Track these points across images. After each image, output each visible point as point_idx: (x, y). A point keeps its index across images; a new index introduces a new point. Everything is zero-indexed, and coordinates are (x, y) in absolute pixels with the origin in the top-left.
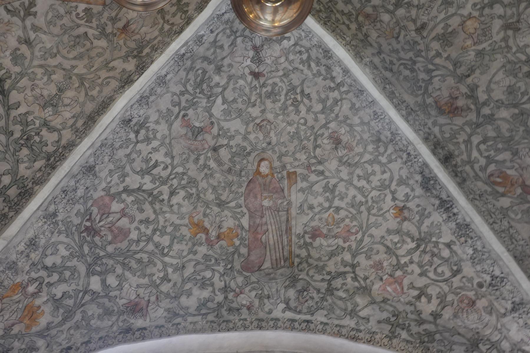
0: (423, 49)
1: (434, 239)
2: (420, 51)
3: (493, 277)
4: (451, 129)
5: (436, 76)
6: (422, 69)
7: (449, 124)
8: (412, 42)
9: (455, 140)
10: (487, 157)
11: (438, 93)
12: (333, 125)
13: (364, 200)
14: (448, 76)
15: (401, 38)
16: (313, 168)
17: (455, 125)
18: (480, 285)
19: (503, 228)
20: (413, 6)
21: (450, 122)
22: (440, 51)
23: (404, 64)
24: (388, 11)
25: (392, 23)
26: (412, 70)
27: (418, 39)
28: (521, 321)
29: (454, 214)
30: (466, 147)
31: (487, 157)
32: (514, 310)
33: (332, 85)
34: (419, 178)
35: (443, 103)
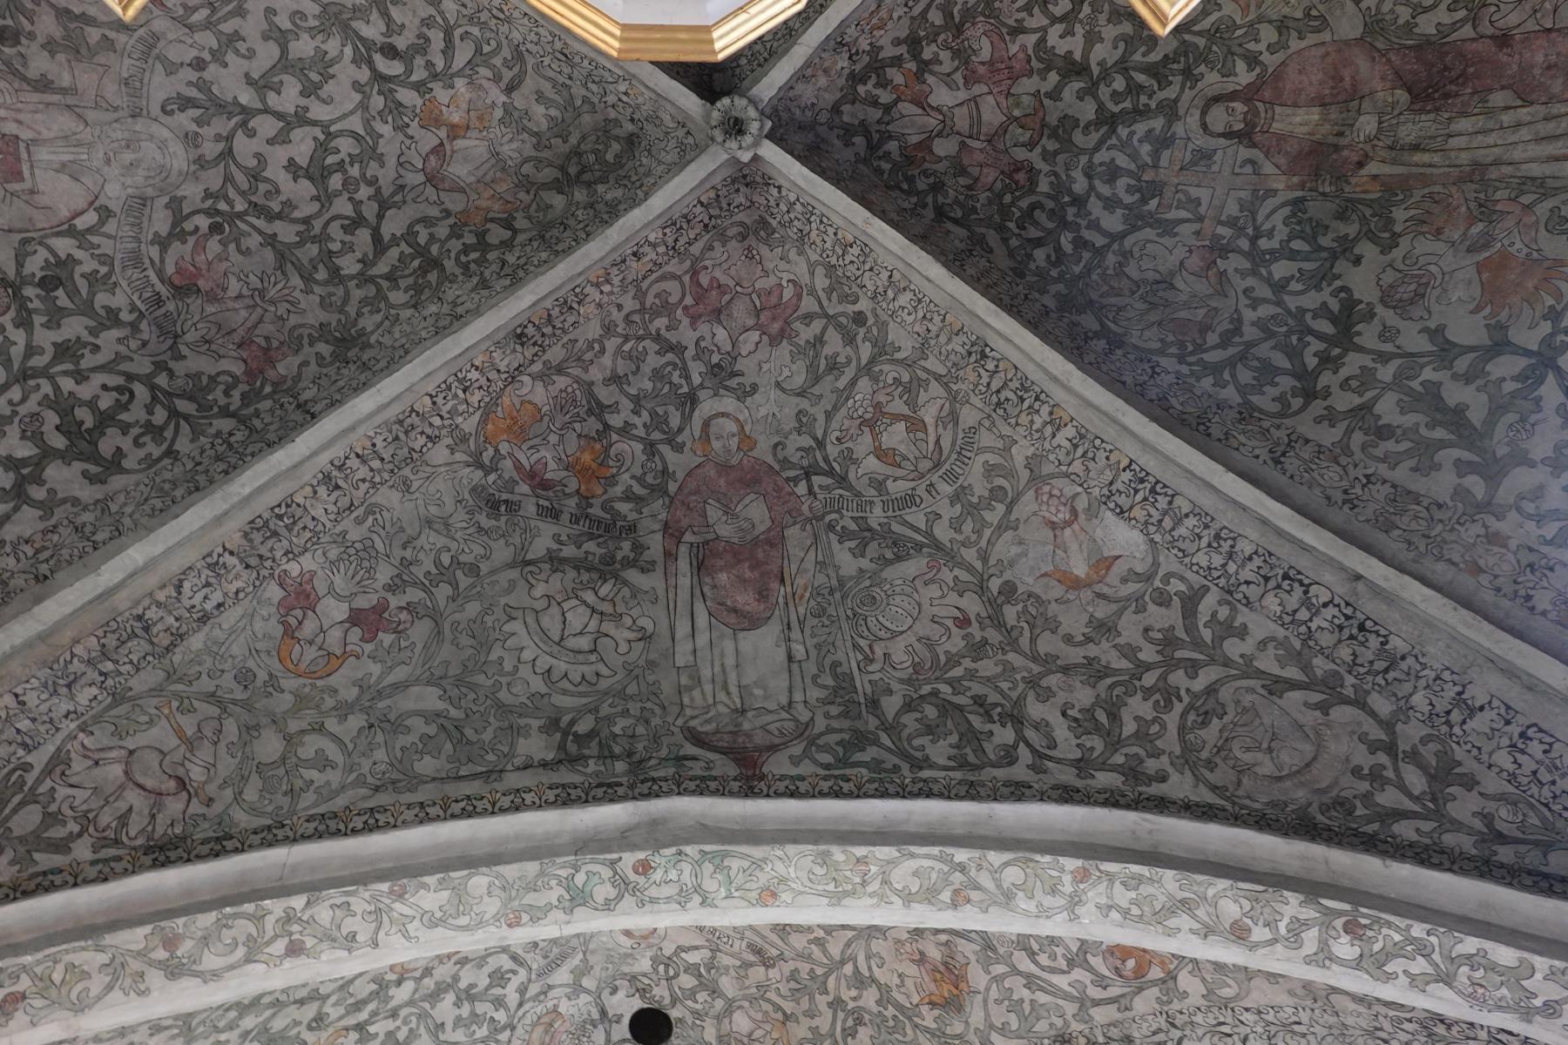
0: (808, 967)
2: (812, 975)
4: (998, 1002)
5: (870, 968)
6: (854, 993)
7: (985, 1001)
8: (793, 985)
9: (1027, 1007)
10: (1071, 963)
11: (909, 983)
14: (868, 946)
15: (788, 1007)
17: (988, 989)
19: (1259, 1029)
20: (713, 958)
21: (979, 997)
22: (812, 937)
23: (844, 1030)
24: (729, 1010)
25: (752, 1013)
26: (859, 1022)
27: (787, 968)
30: (1042, 989)
31: (1071, 963)
35: (933, 987)
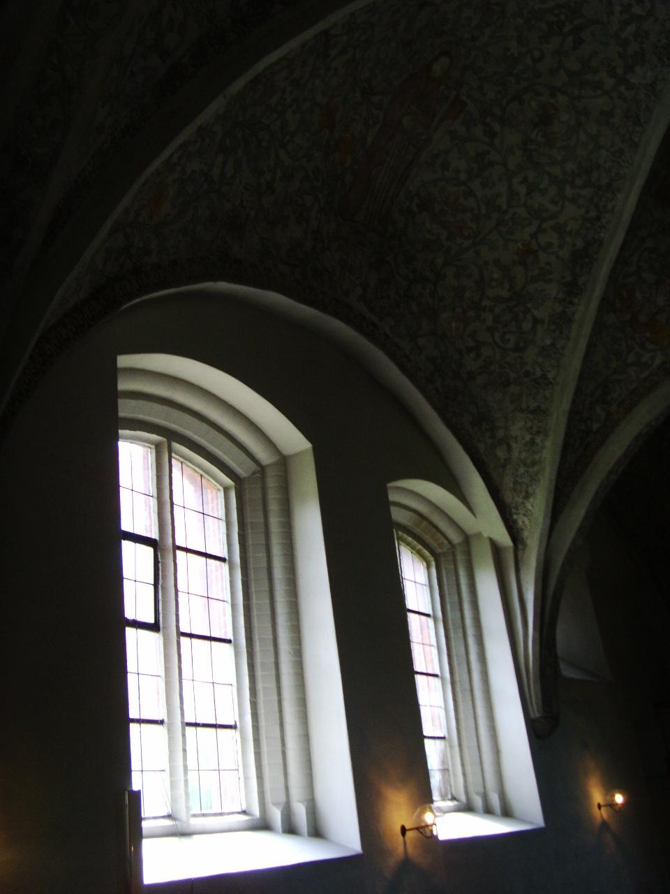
1: (529, 305)
3: (544, 376)
12: (562, 99)
13: (504, 207)
16: (488, 120)
18: (527, 374)
28: (529, 424)
29: (571, 303)
32: (533, 412)
33: (620, 71)
34: (580, 244)
